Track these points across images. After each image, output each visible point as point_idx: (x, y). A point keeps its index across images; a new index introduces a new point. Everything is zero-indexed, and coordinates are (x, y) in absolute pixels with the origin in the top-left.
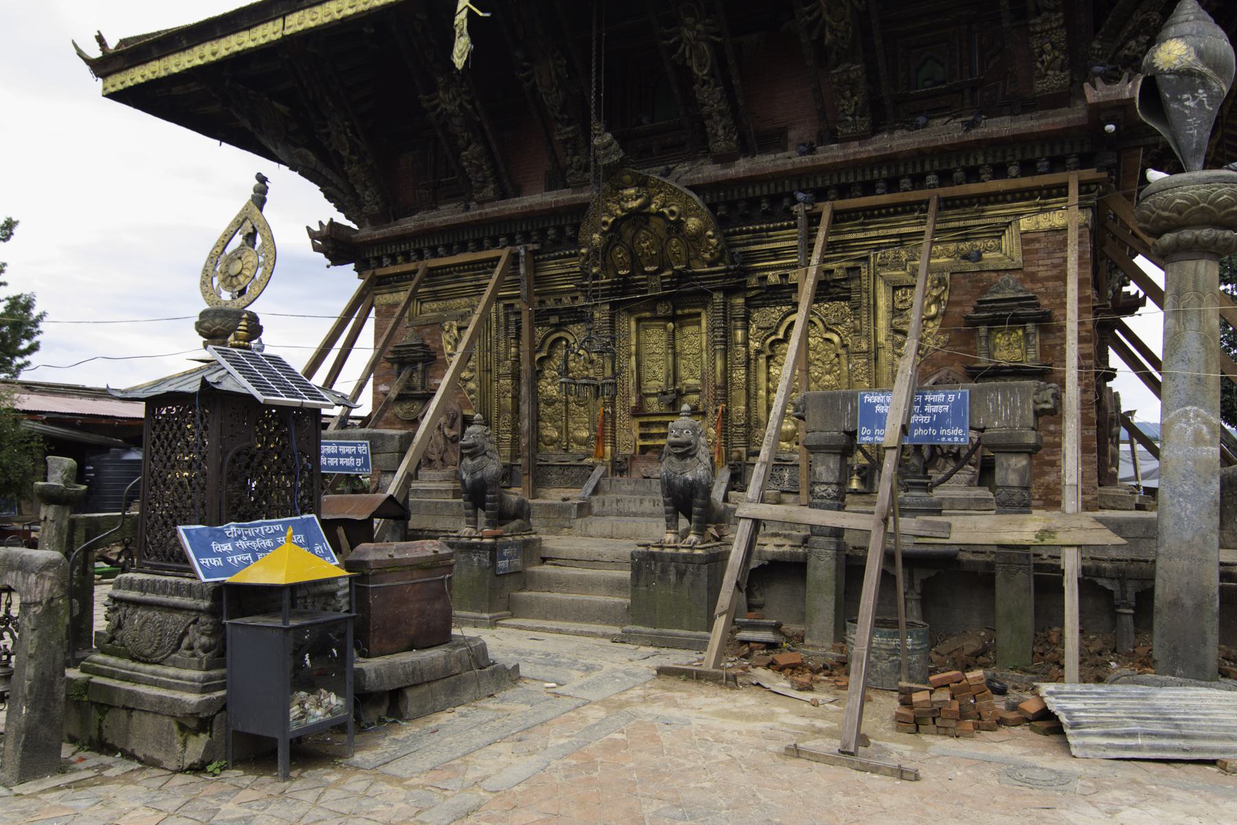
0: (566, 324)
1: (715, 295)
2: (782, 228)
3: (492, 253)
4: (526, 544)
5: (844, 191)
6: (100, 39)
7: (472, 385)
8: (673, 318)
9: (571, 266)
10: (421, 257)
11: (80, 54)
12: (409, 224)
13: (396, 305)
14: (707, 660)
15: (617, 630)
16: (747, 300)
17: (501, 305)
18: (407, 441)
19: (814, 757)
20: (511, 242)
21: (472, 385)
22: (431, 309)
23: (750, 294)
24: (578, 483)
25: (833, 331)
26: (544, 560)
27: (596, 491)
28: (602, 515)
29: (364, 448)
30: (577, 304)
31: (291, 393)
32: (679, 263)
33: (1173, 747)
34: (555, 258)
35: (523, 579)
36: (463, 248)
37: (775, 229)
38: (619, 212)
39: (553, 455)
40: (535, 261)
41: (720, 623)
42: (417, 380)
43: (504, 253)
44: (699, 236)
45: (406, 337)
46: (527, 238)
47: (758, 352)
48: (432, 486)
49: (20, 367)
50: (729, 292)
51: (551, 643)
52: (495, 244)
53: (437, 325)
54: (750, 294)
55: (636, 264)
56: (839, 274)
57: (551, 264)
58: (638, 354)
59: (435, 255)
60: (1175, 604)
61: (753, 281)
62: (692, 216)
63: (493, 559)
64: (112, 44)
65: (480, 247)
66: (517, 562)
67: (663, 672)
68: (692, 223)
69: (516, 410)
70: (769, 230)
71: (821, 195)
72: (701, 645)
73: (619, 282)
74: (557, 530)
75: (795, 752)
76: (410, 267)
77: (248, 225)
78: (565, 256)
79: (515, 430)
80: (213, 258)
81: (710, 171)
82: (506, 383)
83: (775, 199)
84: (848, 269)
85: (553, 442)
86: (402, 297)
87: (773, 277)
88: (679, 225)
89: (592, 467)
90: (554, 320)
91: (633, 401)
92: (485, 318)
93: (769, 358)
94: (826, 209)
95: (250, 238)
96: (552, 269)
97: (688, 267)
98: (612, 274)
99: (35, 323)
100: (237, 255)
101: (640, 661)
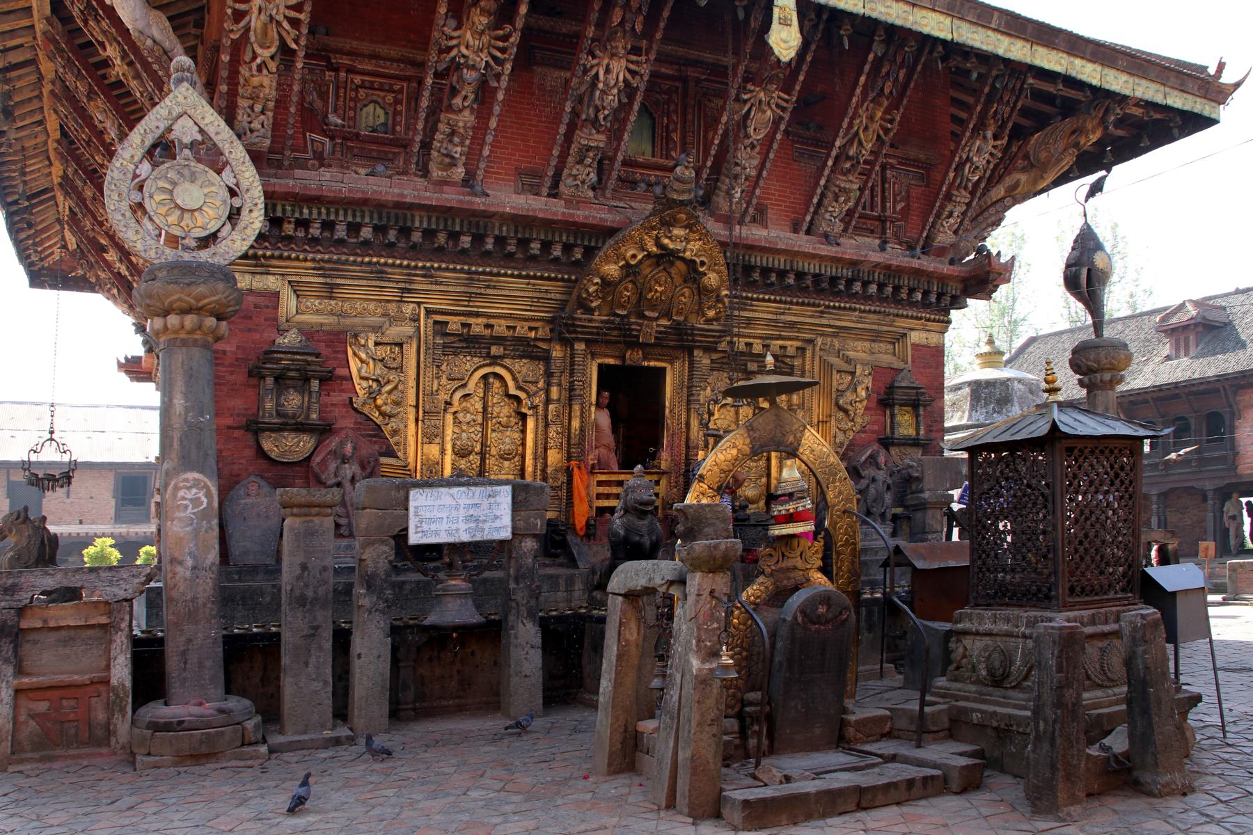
0: (502, 357)
2: (764, 300)
9: (547, 291)
17: (430, 321)
30: (533, 335)
34: (528, 277)
37: (758, 300)
38: (655, 249)
50: (708, 349)
54: (715, 356)
55: (640, 304)
56: (791, 351)
61: (723, 346)
62: (714, 271)
68: (712, 279)
70: (752, 299)
78: (542, 278)
83: (765, 271)
84: (798, 348)
87: (741, 344)
90: (495, 350)
98: (606, 310)
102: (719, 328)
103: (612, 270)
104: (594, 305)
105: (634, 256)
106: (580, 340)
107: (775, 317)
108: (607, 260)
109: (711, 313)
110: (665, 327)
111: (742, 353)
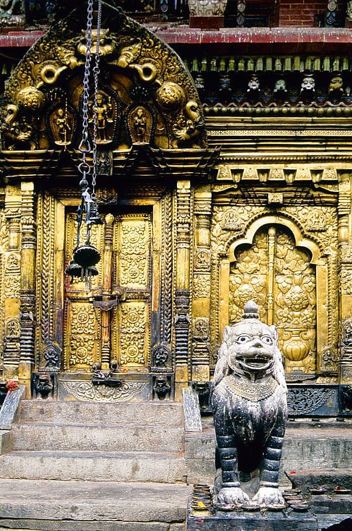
1: (180, 185)
16: (213, 193)
23: (218, 189)
25: (312, 239)
32: (141, 138)
38: (73, 60)
47: (223, 256)
50: (198, 183)
54: (218, 189)
61: (225, 172)
68: (169, 90)
73: (55, 155)
83: (268, 79)
87: (250, 172)
93: (233, 265)
97: (153, 144)
98: (44, 143)
102: (200, 150)
103: (29, 93)
104: (22, 136)
105: (49, 74)
106: (27, 180)
107: (293, 134)
108: (21, 84)
109: (182, 133)
110: (125, 154)
111: (257, 183)
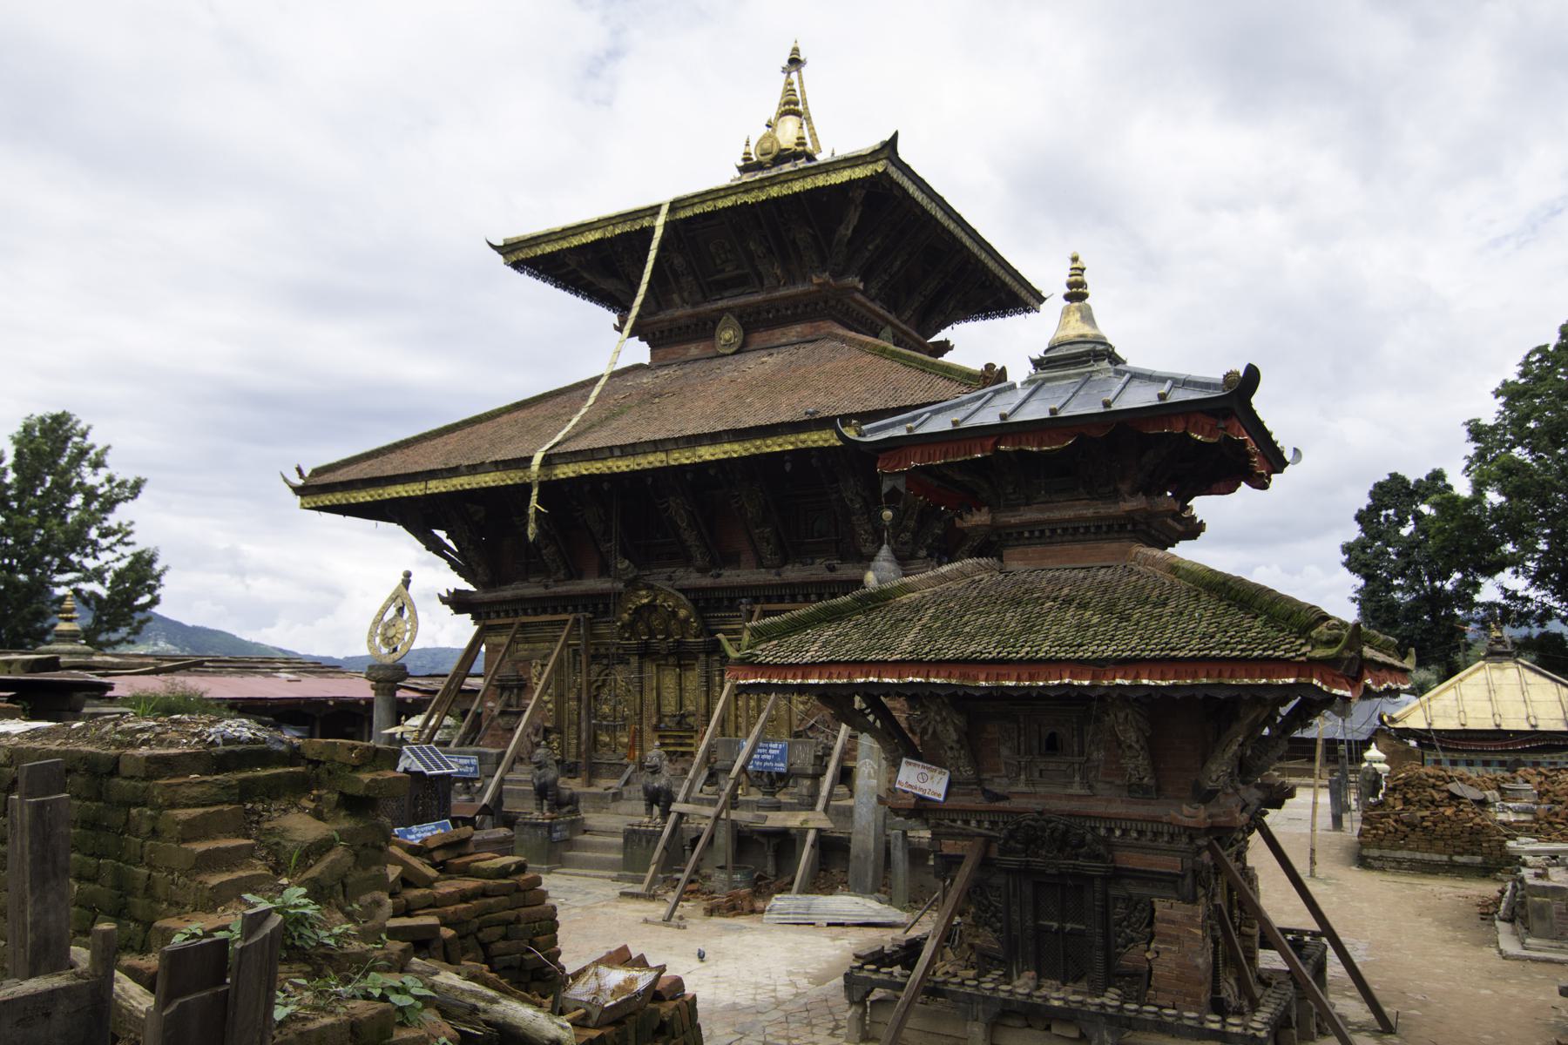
3: (563, 617)
4: (573, 822)
5: (769, 600)
6: (299, 470)
7: (550, 706)
8: (680, 666)
10: (516, 614)
11: (286, 480)
12: (508, 592)
13: (501, 645)
14: (639, 889)
15: (614, 874)
18: (502, 755)
19: (653, 923)
20: (575, 610)
21: (550, 706)
22: (523, 650)
24: (618, 776)
26: (585, 832)
27: (627, 783)
28: (629, 799)
29: (474, 761)
31: (439, 768)
33: (801, 918)
35: (569, 844)
36: (545, 612)
39: (606, 756)
40: (591, 625)
41: (652, 869)
42: (513, 701)
43: (571, 618)
44: (686, 620)
45: (507, 671)
46: (585, 608)
48: (522, 777)
49: (142, 623)
51: (577, 882)
52: (565, 611)
53: (527, 661)
57: (602, 626)
58: (658, 689)
59: (526, 614)
60: (857, 857)
63: (550, 833)
64: (307, 473)
65: (555, 612)
66: (567, 834)
67: (623, 894)
68: (682, 613)
69: (579, 724)
71: (756, 600)
72: (640, 881)
74: (598, 810)
75: (646, 921)
76: (509, 621)
77: (399, 601)
79: (579, 737)
80: (376, 623)
81: (695, 579)
82: (573, 704)
85: (606, 745)
86: (504, 640)
88: (674, 614)
89: (627, 766)
90: (605, 662)
91: (654, 720)
92: (560, 660)
94: (758, 609)
95: (401, 610)
96: (602, 629)
99: (158, 578)
100: (391, 624)
101: (614, 889)
